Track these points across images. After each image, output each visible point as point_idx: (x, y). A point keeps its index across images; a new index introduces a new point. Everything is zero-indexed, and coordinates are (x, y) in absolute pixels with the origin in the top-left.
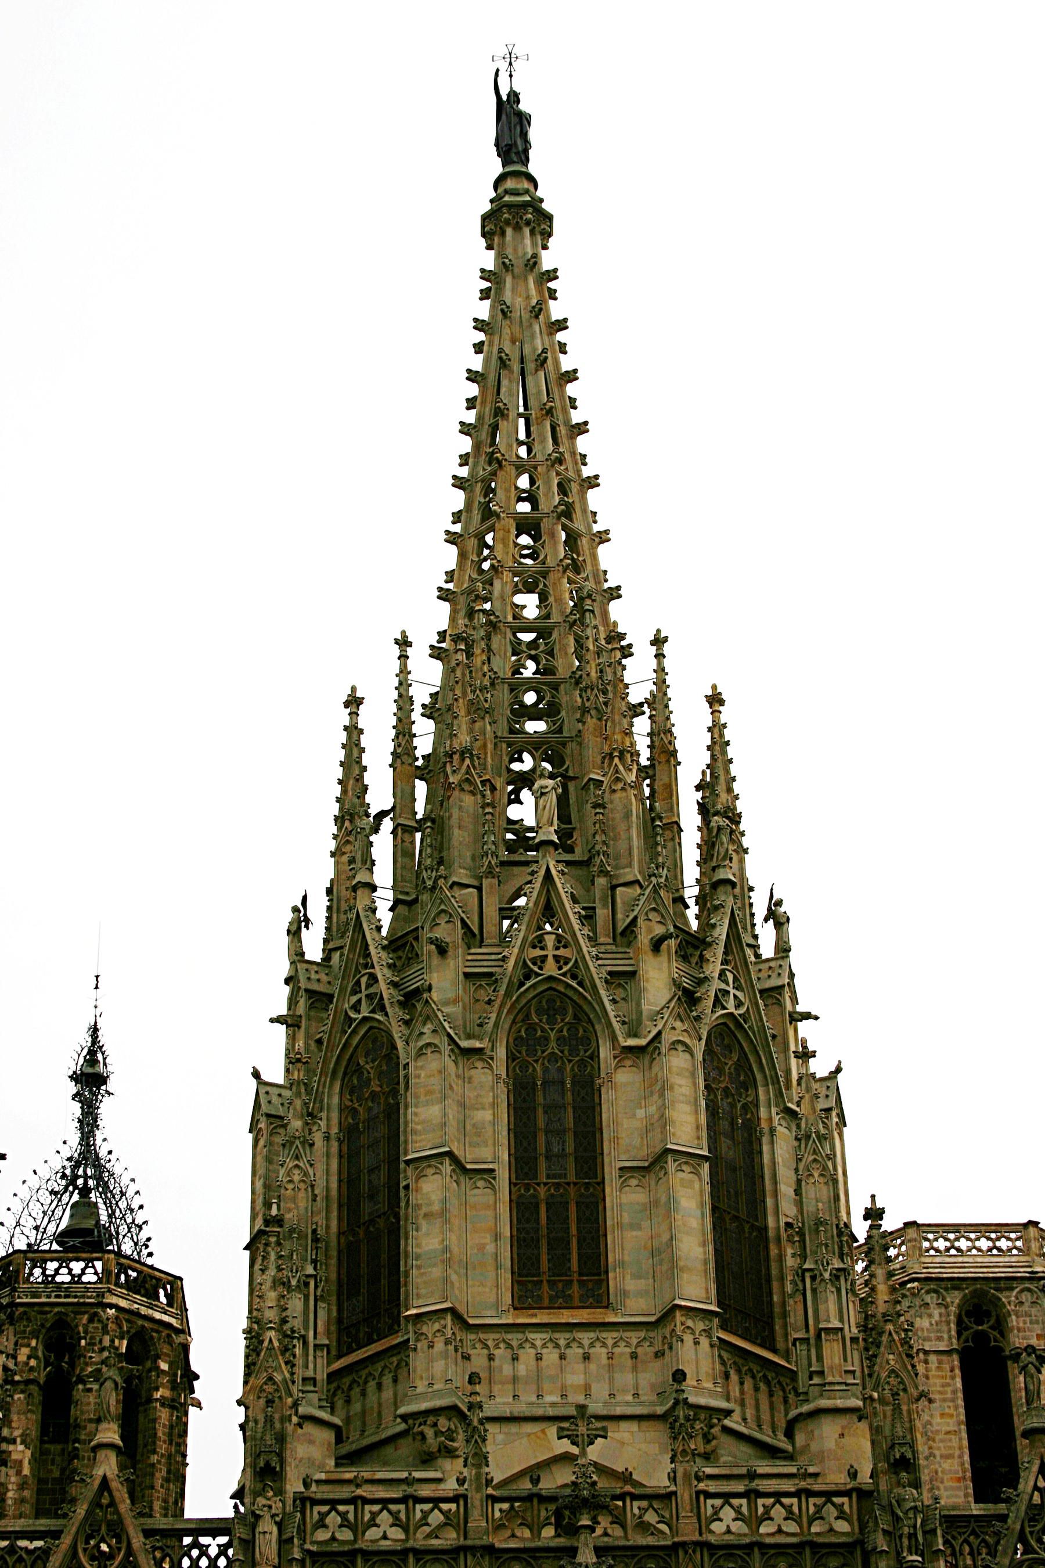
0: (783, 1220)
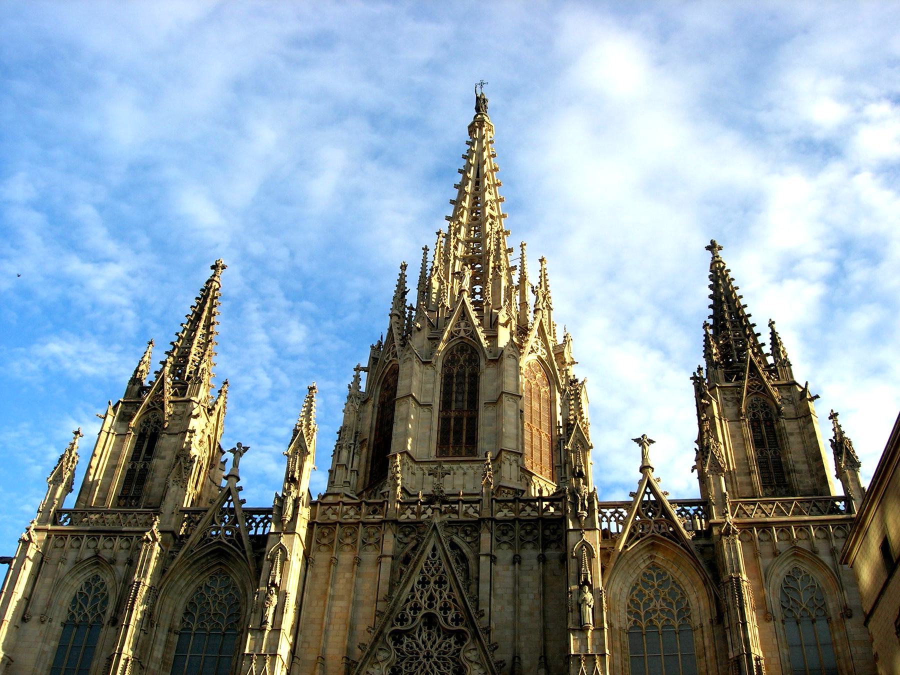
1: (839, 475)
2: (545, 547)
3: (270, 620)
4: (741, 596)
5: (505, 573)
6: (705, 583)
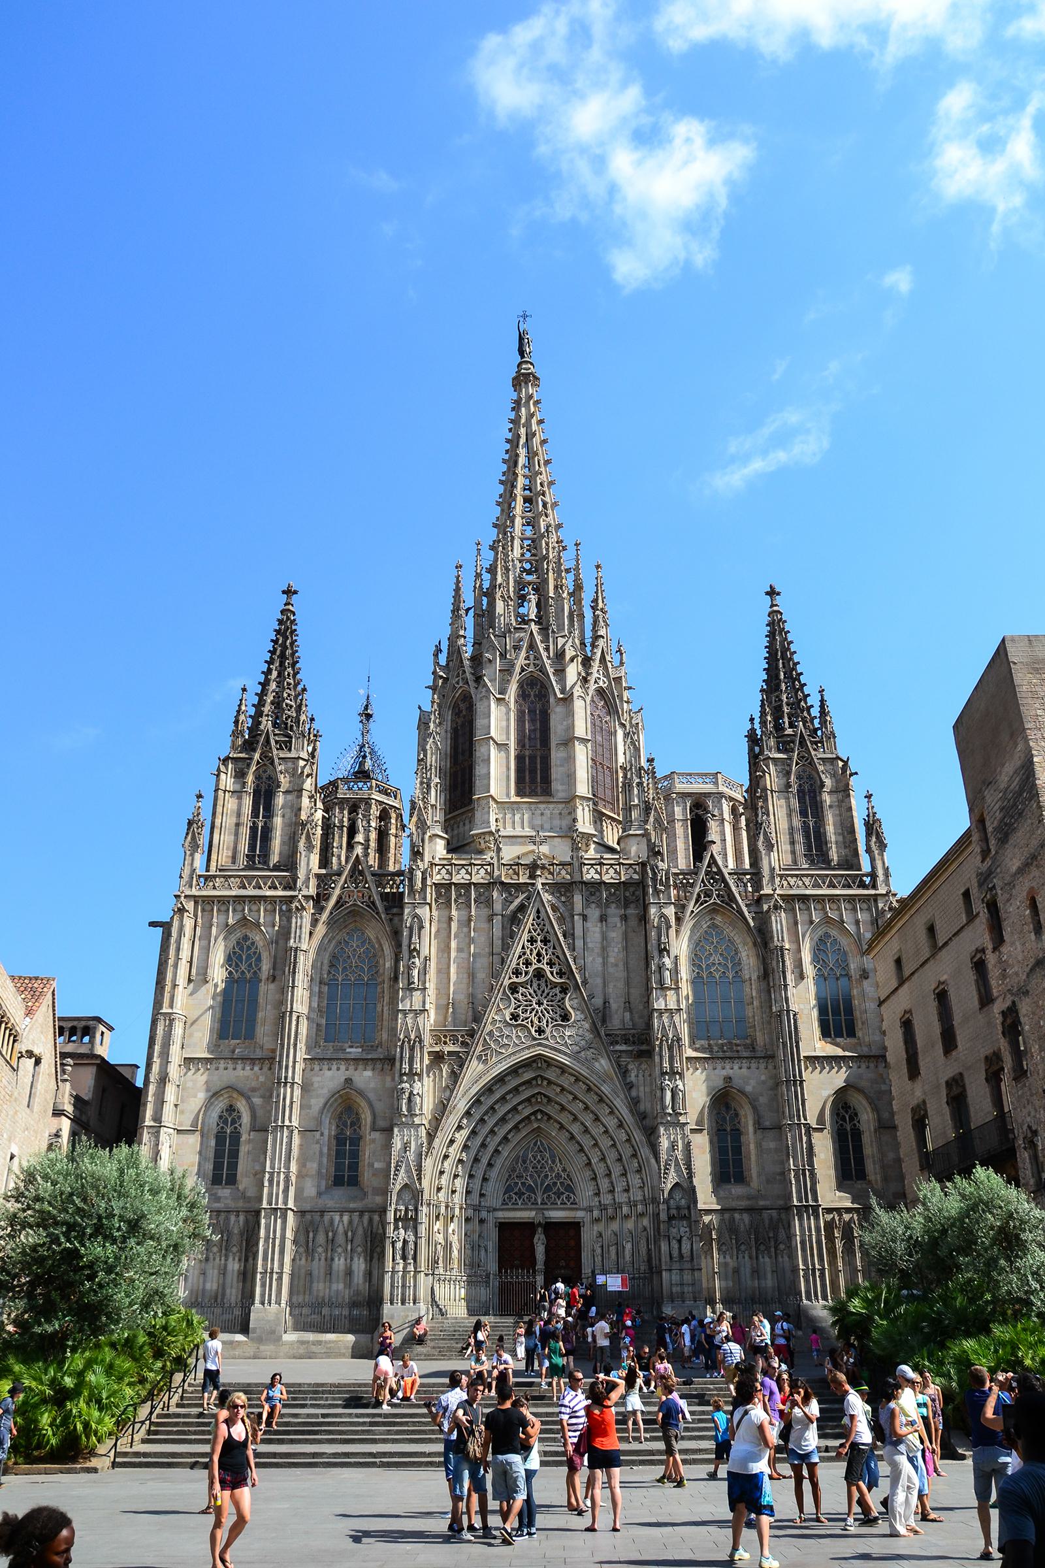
0: (620, 764)
1: (869, 850)
2: (626, 907)
3: (416, 980)
4: (784, 962)
5: (595, 929)
6: (755, 944)
